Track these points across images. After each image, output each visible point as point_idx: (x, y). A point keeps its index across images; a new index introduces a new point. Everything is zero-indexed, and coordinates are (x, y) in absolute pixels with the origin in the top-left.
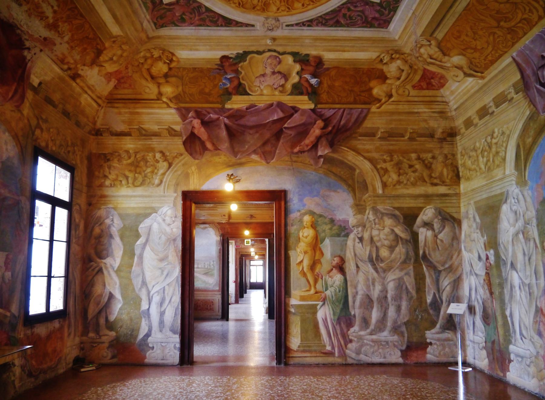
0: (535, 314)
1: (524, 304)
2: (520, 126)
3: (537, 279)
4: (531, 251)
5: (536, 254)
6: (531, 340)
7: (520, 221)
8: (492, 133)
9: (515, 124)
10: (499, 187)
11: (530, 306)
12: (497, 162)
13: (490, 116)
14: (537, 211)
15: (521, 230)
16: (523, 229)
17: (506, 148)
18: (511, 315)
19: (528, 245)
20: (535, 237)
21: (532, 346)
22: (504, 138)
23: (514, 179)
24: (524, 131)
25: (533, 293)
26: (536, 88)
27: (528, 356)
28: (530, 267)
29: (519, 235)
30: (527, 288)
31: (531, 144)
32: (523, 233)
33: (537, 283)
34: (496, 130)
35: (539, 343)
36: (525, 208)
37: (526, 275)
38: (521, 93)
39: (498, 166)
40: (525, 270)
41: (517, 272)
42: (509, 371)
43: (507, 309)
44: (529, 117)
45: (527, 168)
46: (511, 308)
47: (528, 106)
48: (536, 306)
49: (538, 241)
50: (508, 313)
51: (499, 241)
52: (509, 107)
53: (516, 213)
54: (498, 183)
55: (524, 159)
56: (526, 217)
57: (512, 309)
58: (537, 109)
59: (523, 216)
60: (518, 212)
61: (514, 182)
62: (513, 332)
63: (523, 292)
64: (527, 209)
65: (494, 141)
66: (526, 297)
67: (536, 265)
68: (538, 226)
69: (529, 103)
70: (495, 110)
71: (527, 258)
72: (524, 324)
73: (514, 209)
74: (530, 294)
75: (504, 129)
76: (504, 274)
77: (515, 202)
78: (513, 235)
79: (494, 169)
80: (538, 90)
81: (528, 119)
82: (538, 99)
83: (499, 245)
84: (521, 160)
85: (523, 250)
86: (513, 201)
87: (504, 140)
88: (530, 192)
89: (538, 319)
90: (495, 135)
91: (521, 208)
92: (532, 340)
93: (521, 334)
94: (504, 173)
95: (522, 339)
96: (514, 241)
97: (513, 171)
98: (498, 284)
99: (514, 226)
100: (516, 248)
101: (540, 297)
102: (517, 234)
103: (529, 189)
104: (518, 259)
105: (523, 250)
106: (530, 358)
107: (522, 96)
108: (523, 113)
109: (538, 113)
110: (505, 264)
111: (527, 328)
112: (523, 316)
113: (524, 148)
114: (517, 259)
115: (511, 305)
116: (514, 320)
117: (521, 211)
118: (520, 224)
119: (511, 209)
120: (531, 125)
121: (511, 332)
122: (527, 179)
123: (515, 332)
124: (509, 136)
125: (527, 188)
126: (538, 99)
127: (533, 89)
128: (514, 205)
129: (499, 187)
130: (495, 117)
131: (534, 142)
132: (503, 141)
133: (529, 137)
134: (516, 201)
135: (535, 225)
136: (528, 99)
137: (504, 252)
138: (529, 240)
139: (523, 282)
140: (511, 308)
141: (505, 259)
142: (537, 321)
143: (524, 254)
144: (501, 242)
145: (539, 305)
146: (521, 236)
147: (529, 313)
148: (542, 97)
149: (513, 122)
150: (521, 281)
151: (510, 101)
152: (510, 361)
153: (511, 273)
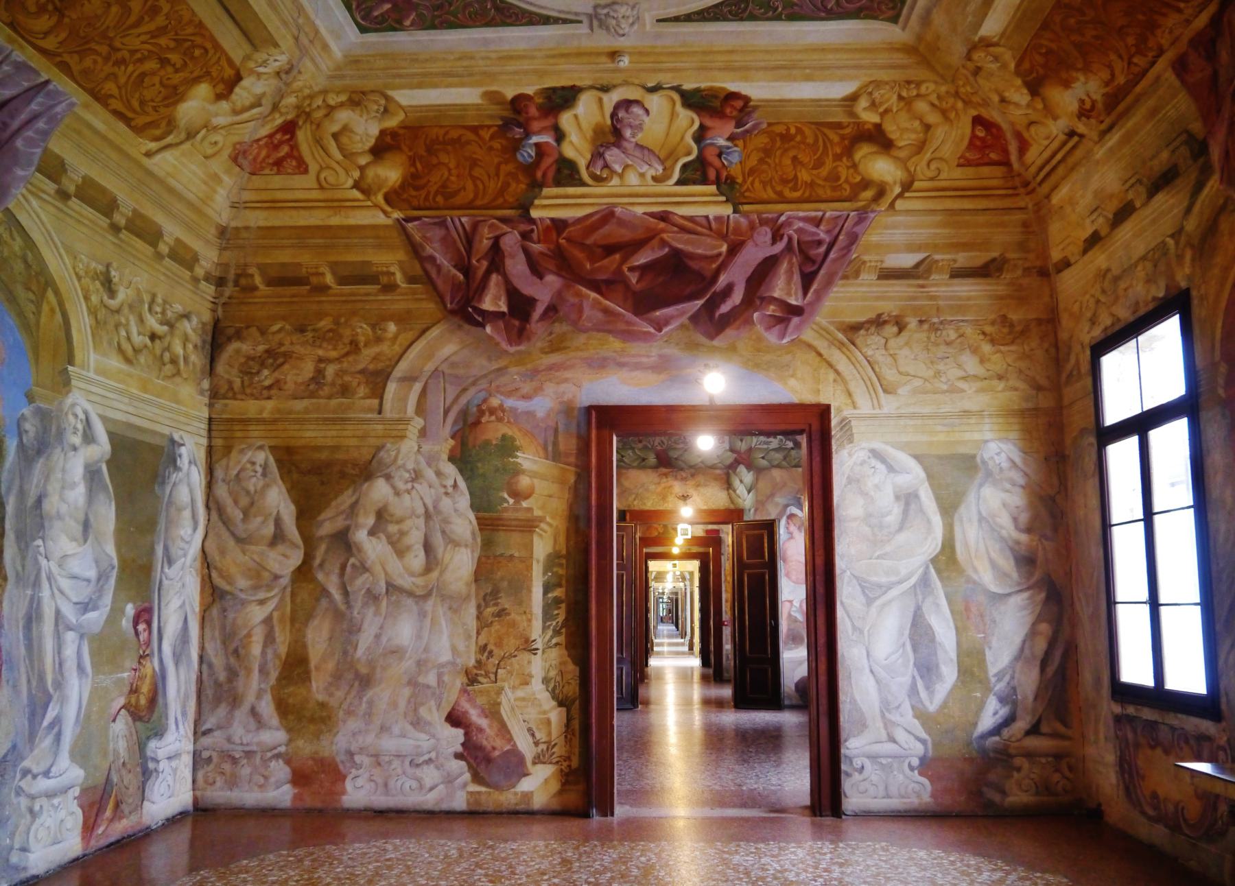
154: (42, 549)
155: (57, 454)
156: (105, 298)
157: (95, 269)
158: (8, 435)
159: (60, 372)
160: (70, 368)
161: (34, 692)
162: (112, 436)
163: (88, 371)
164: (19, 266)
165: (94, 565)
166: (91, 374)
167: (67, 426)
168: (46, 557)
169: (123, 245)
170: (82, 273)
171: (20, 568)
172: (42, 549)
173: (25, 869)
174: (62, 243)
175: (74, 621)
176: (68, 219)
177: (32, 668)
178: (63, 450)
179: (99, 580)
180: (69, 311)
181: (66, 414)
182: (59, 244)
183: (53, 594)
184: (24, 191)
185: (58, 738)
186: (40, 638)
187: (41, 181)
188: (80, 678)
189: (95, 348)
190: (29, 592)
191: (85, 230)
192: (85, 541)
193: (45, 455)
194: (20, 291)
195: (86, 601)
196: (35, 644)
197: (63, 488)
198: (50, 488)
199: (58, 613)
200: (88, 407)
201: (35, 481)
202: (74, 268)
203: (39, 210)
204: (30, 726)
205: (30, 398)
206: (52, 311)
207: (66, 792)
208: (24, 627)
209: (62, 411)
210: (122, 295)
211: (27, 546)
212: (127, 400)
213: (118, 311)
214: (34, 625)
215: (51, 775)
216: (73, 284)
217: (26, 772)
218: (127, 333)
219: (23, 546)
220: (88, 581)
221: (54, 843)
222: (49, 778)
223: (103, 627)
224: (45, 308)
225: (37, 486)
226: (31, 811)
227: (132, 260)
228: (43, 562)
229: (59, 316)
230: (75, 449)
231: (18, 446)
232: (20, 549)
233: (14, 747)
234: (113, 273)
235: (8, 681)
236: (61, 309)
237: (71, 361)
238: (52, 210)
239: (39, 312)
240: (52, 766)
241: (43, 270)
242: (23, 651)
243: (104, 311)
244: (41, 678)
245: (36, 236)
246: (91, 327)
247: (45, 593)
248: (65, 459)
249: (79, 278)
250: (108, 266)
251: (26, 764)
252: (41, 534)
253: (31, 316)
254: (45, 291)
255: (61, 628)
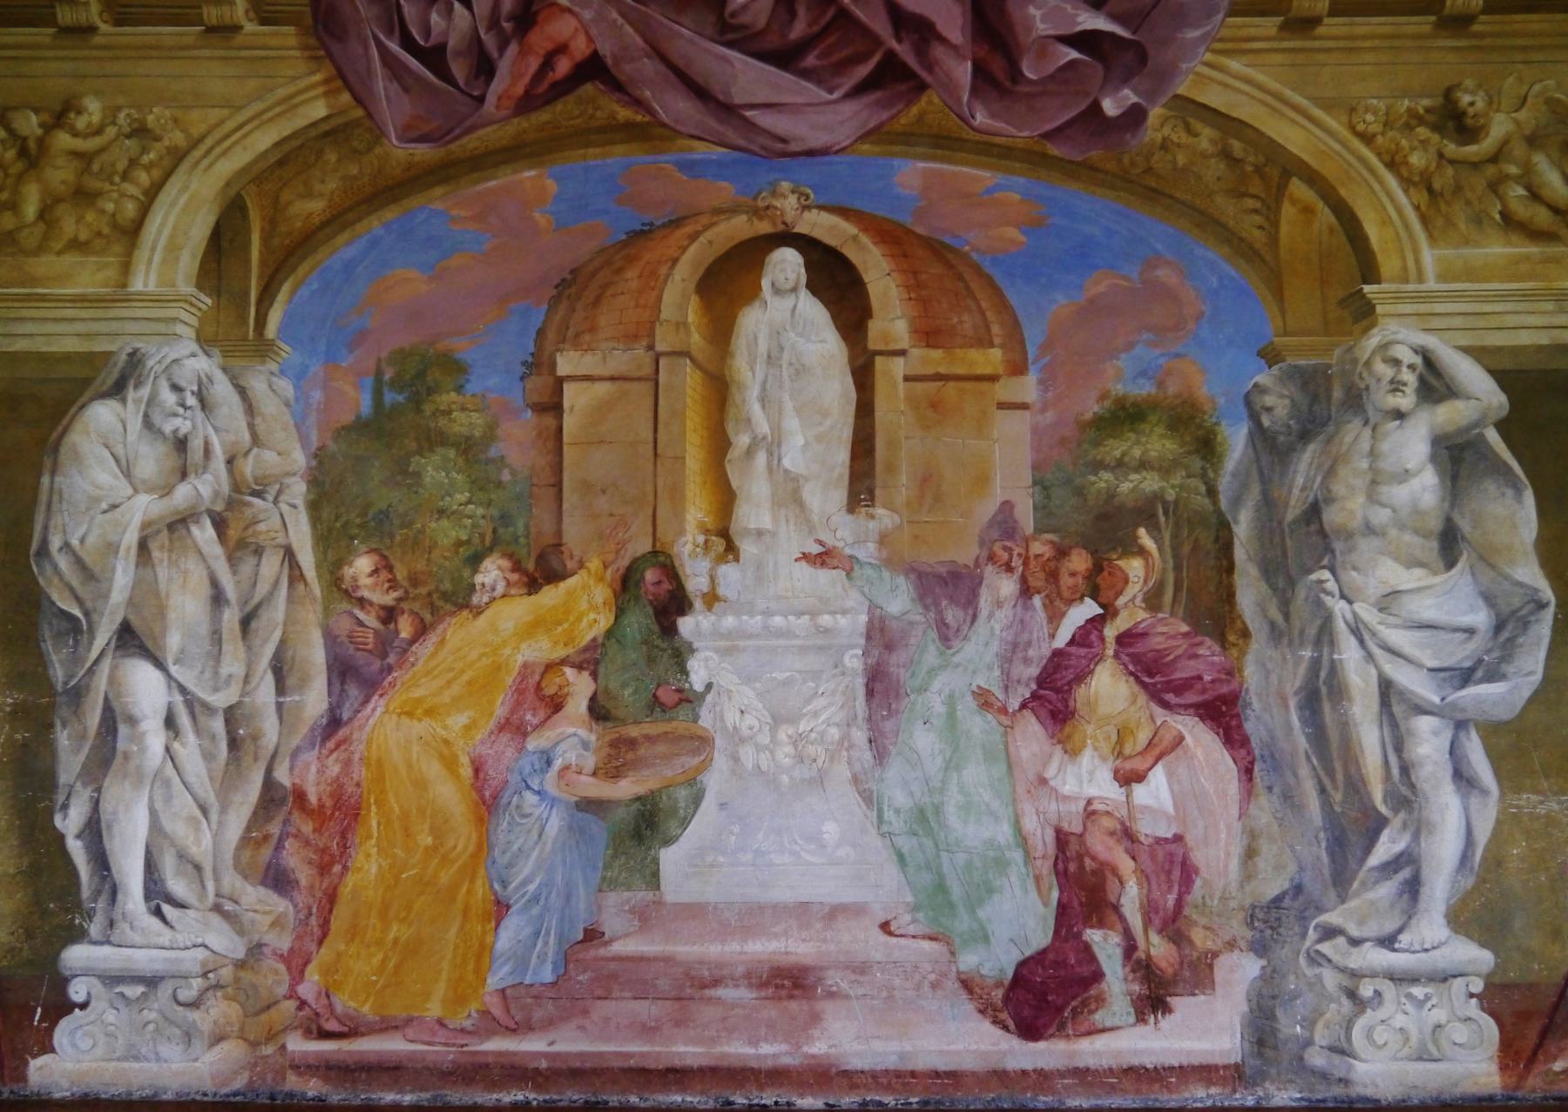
0: (255, 813)
1: (191, 779)
2: (264, 140)
3: (281, 689)
4: (262, 589)
5: (290, 599)
6: (217, 908)
7: (208, 477)
8: (59, 108)
9: (230, 125)
10: (79, 327)
11: (228, 781)
12: (69, 226)
13: (55, 36)
14: (319, 456)
15: (210, 513)
16: (219, 507)
17: (153, 192)
18: (94, 831)
19: (247, 568)
20: (295, 546)
21: (225, 926)
22: (145, 150)
23: (194, 321)
24: (281, 163)
25: (255, 738)
26: (380, 46)
27: (198, 969)
28: (249, 648)
29: (194, 529)
30: (218, 725)
31: (316, 220)
32: (220, 525)
33: (279, 706)
34: (94, 109)
35: (270, 912)
36: (247, 436)
37: (216, 673)
38: (291, 29)
39: (75, 245)
40: (217, 657)
41: (160, 665)
42: (48, 1048)
43: (65, 807)
44: (325, 127)
45: (282, 297)
46: (96, 804)
47: (321, 90)
48: (269, 784)
49: (307, 559)
50: (70, 822)
51: (45, 543)
52: (207, 52)
53: (181, 444)
54: (69, 313)
55: (263, 263)
56: (248, 468)
57: (106, 807)
58: (370, 116)
59: (230, 462)
60: (196, 444)
61: (191, 333)
62: (97, 894)
63: (190, 737)
64: (256, 440)
65: (63, 140)
66: (208, 756)
67: (283, 642)
68: (314, 507)
69: (326, 81)
70: (104, 27)
71: (231, 618)
72: (182, 856)
73: (168, 428)
74: (234, 744)
75: (150, 118)
76: (58, 673)
77: (183, 405)
78: (145, 525)
79: (40, 250)
80: (388, 59)
81: (313, 133)
82: (381, 84)
83: (43, 551)
84: (248, 261)
85: (214, 583)
86: (169, 398)
87: (146, 159)
88: (286, 387)
89: (275, 829)
90: (81, 123)
91: (216, 429)
92: (228, 906)
93: (157, 895)
94: (124, 285)
95: (158, 913)
96: (153, 546)
97: (186, 288)
98: (14, 713)
99: (167, 491)
100: (163, 573)
101: (295, 755)
102: (179, 523)
103: (282, 372)
104: (172, 616)
105: (214, 583)
106: (205, 975)
107: (293, 41)
108: (289, 105)
109: (379, 134)
110: (74, 630)
111: (198, 868)
112: (177, 828)
113: (271, 224)
114: (161, 612)
115: (99, 790)
116: (113, 845)
117: (215, 440)
118: (206, 491)
119: (148, 423)
120: (331, 157)
121: (86, 893)
122: (271, 331)
123: (111, 889)
124: (177, 157)
125: (273, 366)
126: (381, 84)
127: (366, 47)
128: (176, 415)
129: (79, 327)
130: (95, 53)
131: (339, 219)
132: (133, 163)
133: (309, 195)
134: (191, 401)
135: (300, 502)
136: (327, 70)
137: (75, 583)
138: (259, 552)
139: (191, 702)
140: (96, 804)
141: (77, 612)
142: (266, 838)
143: (218, 599)
144: (55, 543)
145: (283, 775)
146: (204, 533)
147: (224, 810)
148: (406, 90)
149: (226, 112)
150: (178, 699)
151: (211, 30)
152: (62, 1007)
153: (114, 668)
154: (1331, 585)
155: (1353, 433)
156: (1451, 149)
157: (1409, 110)
158: (1223, 423)
159: (1342, 303)
160: (1367, 288)
161: (1338, 809)
162: (1502, 377)
163: (1421, 279)
164: (1216, 168)
165: (1480, 603)
166: (1431, 284)
167: (1372, 382)
168: (1343, 597)
169: (1487, 42)
170: (1373, 128)
171: (1279, 619)
172: (1331, 585)
173: (1345, 1082)
174: (1308, 98)
175: (1437, 700)
176: (1321, 57)
177: (1331, 774)
178: (1366, 423)
179: (1499, 628)
180: (1350, 201)
181: (1368, 364)
182: (1304, 103)
183: (1370, 657)
184: (1208, 57)
185: (1413, 888)
186: (1345, 726)
187: (1240, 27)
188: (1465, 798)
189: (1431, 237)
190: (1307, 653)
191: (1370, 57)
192: (1450, 564)
193: (1320, 438)
194: (1227, 208)
195: (1467, 664)
196: (1333, 735)
197: (1374, 482)
198: (1338, 488)
199: (1386, 688)
200: (1431, 341)
201: (1300, 480)
202: (1353, 129)
203: (1250, 72)
204: (1333, 860)
205: (1270, 356)
206: (1308, 210)
207: (1445, 980)
208: (1301, 708)
209: (1355, 361)
210: (1499, 127)
211: (1292, 583)
212: (1550, 306)
213: (1494, 159)
214: (1327, 707)
215: (1397, 946)
216: (1353, 152)
217: (1330, 933)
218: (1528, 188)
219: (1281, 583)
220: (1470, 631)
221: (1420, 1059)
222: (1395, 950)
223: (1525, 709)
224: (1288, 211)
225: (1304, 489)
226: (1352, 994)
227: (1519, 57)
228: (1339, 607)
229: (1325, 216)
230: (1399, 415)
231: (1251, 433)
232: (1274, 588)
233: (1298, 889)
234: (1466, 99)
235: (1270, 789)
236: (1327, 203)
237: (1370, 272)
238: (1278, 58)
239: (1275, 224)
240: (1400, 930)
241: (1271, 151)
242: (1302, 743)
243: (1450, 171)
244: (1356, 786)
245: (1246, 111)
246: (1417, 208)
247: (1349, 653)
248: (1373, 437)
249: (1368, 139)
250: (1448, 93)
251: (1332, 918)
252: (1325, 562)
253: (1257, 233)
254: (1282, 187)
255: (1397, 709)
